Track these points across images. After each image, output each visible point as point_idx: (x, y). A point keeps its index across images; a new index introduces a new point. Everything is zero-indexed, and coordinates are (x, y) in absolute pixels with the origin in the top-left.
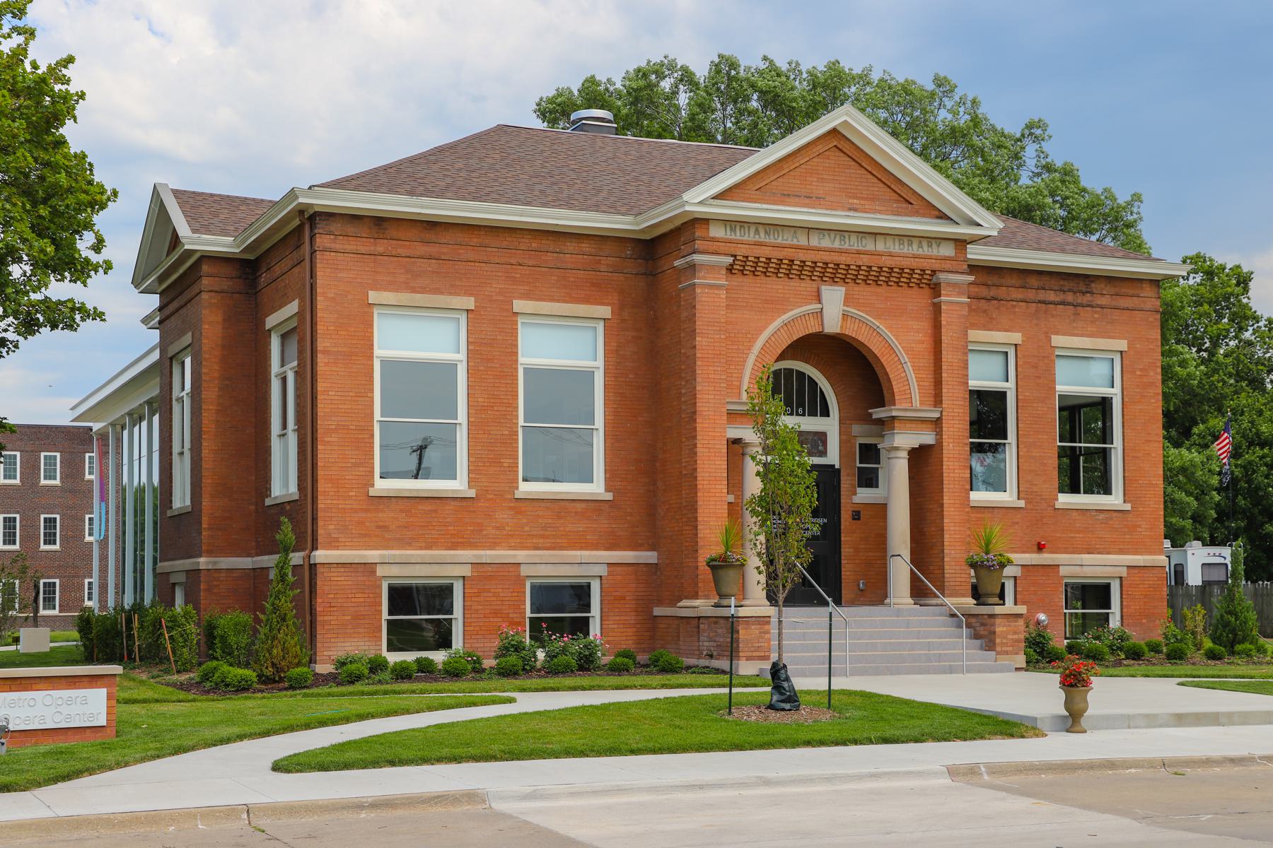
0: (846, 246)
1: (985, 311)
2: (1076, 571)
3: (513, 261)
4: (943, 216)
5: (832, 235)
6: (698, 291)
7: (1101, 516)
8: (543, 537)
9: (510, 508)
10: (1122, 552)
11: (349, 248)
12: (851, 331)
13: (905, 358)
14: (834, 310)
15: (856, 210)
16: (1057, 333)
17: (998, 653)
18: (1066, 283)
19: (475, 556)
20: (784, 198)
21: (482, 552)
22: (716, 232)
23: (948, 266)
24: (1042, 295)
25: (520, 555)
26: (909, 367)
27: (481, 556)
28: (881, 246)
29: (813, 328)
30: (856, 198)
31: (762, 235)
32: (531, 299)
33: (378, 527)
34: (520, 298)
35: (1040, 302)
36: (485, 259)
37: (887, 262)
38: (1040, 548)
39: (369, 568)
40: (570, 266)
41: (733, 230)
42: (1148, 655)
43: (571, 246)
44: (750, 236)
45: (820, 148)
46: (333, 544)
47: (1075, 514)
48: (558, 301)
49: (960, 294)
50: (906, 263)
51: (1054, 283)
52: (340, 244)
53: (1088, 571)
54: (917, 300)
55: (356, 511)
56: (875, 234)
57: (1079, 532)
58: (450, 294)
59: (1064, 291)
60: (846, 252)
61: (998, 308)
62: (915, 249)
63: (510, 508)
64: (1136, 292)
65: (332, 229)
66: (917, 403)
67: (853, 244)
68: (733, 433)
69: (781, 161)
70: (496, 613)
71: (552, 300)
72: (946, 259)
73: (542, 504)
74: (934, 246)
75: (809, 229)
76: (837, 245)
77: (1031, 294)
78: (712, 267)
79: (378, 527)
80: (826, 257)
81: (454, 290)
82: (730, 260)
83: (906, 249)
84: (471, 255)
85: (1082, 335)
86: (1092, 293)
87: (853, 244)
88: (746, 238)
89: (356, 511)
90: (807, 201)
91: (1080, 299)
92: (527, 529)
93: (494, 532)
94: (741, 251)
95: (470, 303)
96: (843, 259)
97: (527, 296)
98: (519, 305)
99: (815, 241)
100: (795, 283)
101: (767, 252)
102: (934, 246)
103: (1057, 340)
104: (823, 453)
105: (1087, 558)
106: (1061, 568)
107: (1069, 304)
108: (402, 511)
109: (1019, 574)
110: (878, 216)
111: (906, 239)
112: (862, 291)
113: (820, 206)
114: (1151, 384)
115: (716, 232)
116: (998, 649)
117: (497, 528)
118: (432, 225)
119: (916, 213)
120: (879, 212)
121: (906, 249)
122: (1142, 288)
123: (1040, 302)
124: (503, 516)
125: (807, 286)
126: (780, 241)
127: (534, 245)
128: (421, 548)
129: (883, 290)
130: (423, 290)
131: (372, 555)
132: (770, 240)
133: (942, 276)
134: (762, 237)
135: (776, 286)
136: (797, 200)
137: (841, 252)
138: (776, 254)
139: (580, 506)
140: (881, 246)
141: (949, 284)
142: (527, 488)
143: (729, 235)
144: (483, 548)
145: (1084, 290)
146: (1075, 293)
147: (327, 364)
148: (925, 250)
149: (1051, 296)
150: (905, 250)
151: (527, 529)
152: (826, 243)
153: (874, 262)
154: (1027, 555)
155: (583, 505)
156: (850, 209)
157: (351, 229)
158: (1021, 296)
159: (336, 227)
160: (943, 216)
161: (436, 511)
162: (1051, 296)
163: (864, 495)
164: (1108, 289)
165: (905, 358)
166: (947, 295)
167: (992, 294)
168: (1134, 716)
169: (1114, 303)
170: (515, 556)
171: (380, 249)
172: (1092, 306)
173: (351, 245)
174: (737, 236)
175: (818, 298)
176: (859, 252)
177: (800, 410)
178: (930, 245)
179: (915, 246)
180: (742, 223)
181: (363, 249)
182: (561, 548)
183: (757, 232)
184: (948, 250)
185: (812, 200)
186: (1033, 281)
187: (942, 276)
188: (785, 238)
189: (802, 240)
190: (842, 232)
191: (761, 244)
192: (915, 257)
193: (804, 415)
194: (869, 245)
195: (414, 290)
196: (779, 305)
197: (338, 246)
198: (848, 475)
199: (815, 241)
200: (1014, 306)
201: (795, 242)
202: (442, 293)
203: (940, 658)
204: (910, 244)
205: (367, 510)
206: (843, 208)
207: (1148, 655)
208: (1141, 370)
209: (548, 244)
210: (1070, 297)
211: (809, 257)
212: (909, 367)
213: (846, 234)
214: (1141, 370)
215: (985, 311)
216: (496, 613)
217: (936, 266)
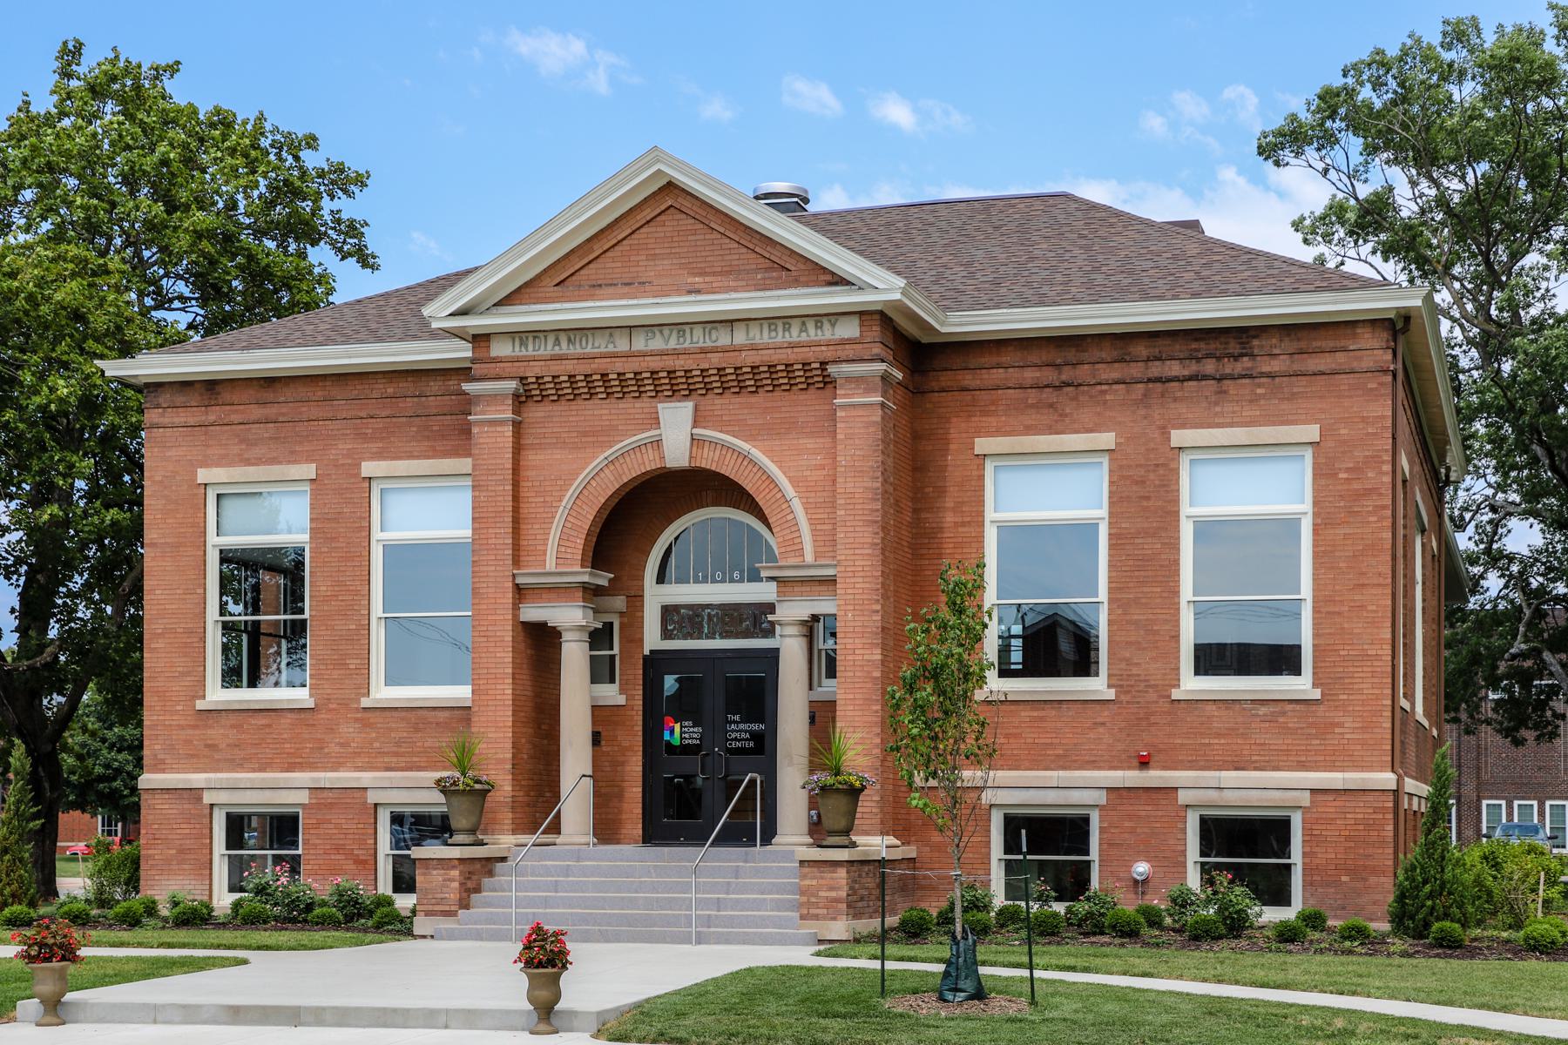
0: (686, 345)
1: (1051, 406)
2: (1213, 795)
3: (363, 414)
4: (837, 280)
5: (666, 331)
6: (475, 430)
7: (1263, 710)
8: (396, 754)
9: (356, 720)
10: (1302, 766)
11: (177, 420)
12: (708, 460)
13: (790, 491)
14: (676, 436)
15: (698, 292)
16: (1183, 426)
18: (1202, 345)
19: (313, 779)
20: (595, 289)
21: (322, 775)
22: (500, 349)
23: (849, 351)
24: (1156, 369)
25: (365, 778)
26: (797, 505)
27: (318, 779)
28: (740, 337)
29: (649, 463)
30: (701, 274)
31: (564, 344)
32: (385, 458)
33: (207, 746)
34: (372, 459)
35: (1150, 380)
36: (330, 415)
37: (749, 358)
38: (1144, 763)
39: (195, 793)
40: (434, 411)
41: (523, 343)
42: (1146, 931)
43: (435, 386)
44: (548, 348)
45: (648, 213)
46: (160, 767)
47: (1210, 708)
48: (418, 457)
49: (868, 391)
51: (1179, 348)
52: (171, 417)
53: (1231, 797)
54: (806, 405)
55: (181, 727)
56: (730, 323)
57: (1218, 735)
58: (289, 462)
59: (1198, 360)
61: (1075, 399)
62: (795, 335)
63: (356, 720)
64: (1343, 343)
65: (161, 400)
66: (809, 557)
67: (699, 339)
68: (531, 613)
69: (589, 240)
70: (338, 849)
71: (411, 457)
72: (843, 342)
73: (395, 714)
74: (827, 326)
75: (630, 329)
76: (673, 344)
77: (1135, 370)
78: (494, 398)
79: (207, 746)
80: (655, 363)
81: (294, 458)
83: (781, 337)
84: (315, 412)
85: (1231, 425)
86: (1252, 356)
87: (699, 339)
89: (181, 727)
90: (626, 289)
91: (1229, 367)
92: (377, 745)
93: (337, 749)
94: (532, 372)
95: (310, 470)
96: (680, 363)
97: (380, 455)
98: (368, 468)
99: (640, 343)
100: (628, 405)
101: (570, 367)
102: (827, 326)
103: (1179, 437)
105: (1229, 777)
106: (1180, 792)
107: (1205, 377)
108: (233, 726)
109: (1103, 801)
110: (734, 295)
111: (780, 323)
112: (716, 403)
113: (645, 294)
114: (1368, 492)
115: (500, 349)
117: (342, 745)
118: (270, 382)
119: (796, 283)
120: (735, 290)
121: (781, 337)
122: (1355, 336)
123: (1150, 380)
124: (348, 730)
125: (644, 404)
126: (589, 350)
127: (390, 390)
128: (254, 771)
129: (760, 399)
130: (258, 462)
131: (197, 779)
132: (576, 350)
133: (831, 369)
134: (564, 348)
135: (599, 411)
136: (611, 290)
137: (676, 353)
138: (582, 369)
139: (442, 715)
140: (740, 337)
141: (849, 379)
142: (383, 693)
143: (519, 352)
144: (325, 769)
145: (1237, 352)
146: (1219, 359)
147: (154, 559)
148: (812, 334)
149: (1175, 369)
150: (779, 339)
151: (377, 745)
152: (657, 343)
153: (729, 361)
154: (1119, 773)
155: (447, 714)
156: (690, 292)
157: (180, 399)
158: (1115, 375)
159: (164, 398)
160: (837, 280)
161: (269, 726)
162: (1175, 369)
163: (610, 694)
164: (1289, 345)
165: (790, 491)
166: (845, 396)
167: (1064, 377)
168: (163, 1006)
169: (1296, 367)
170: (358, 779)
171: (212, 418)
172: (1251, 377)
173: (181, 417)
174: (530, 351)
175: (656, 422)
176: (704, 351)
177: (736, 575)
178: (819, 326)
179: (795, 331)
180: (537, 333)
181: (192, 421)
182: (419, 769)
183: (557, 342)
184: (849, 329)
185: (633, 286)
186: (1141, 350)
187: (831, 369)
188: (599, 345)
189: (622, 345)
190: (680, 326)
191: (560, 358)
192: (792, 346)
193: (741, 580)
194: (723, 338)
195: (248, 462)
196: (600, 436)
197: (166, 421)
199: (640, 343)
200: (1104, 392)
201: (611, 348)
202: (280, 463)
203: (731, 922)
204: (787, 328)
205: (195, 727)
206: (679, 292)
207: (1146, 931)
208: (1348, 470)
209: (406, 386)
210: (1209, 367)
211: (629, 367)
212: (797, 505)
213: (687, 328)
214: (1348, 470)
215: (1051, 406)
216: (338, 849)
217: (828, 354)
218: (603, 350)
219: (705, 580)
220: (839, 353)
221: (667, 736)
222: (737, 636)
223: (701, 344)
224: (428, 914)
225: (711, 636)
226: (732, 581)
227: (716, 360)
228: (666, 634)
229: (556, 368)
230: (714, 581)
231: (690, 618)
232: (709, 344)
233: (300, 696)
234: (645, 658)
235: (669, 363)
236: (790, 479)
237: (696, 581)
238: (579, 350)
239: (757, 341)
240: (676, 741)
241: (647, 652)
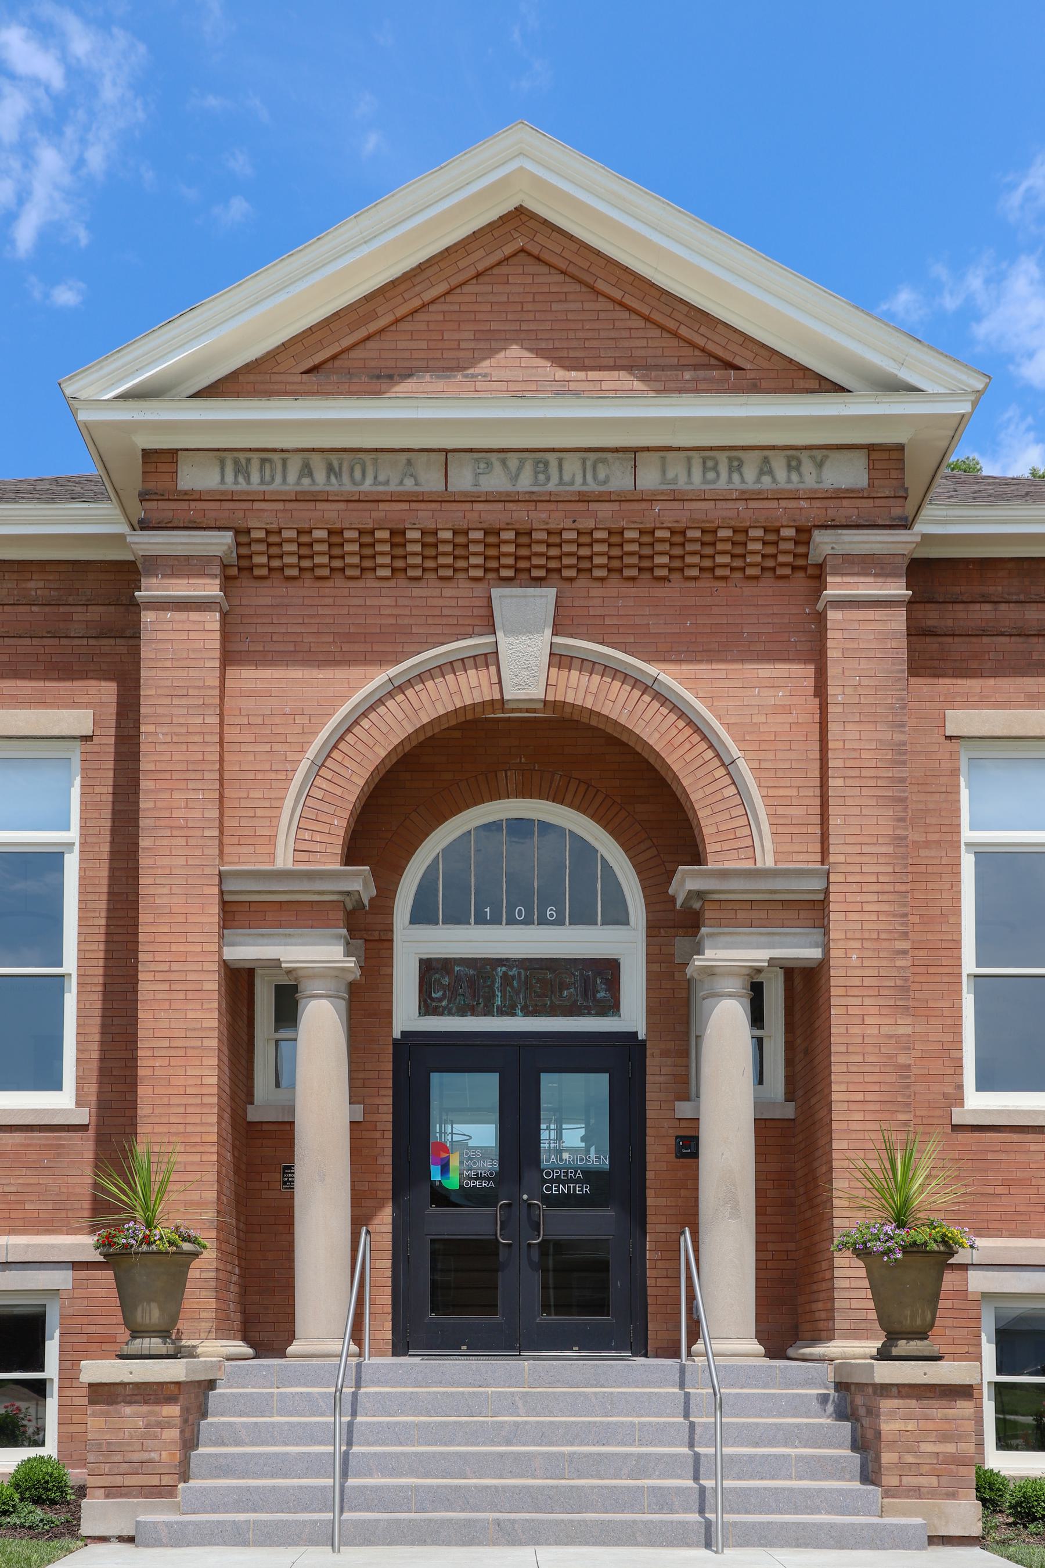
0: (551, 486)
17: (888, 1493)
29: (471, 689)
37: (671, 515)
50: (719, 513)
60: (551, 499)
80: (493, 515)
82: (228, 537)
88: (277, 485)
94: (259, 521)
96: (540, 517)
101: (332, 514)
104: (611, 1007)
116: (890, 1480)
126: (367, 486)
137: (533, 500)
152: (496, 481)
176: (584, 498)
192: (746, 497)
198: (665, 1054)
218: (393, 487)
219: (496, 921)
220: (831, 513)
221: (436, 1175)
222: (553, 1011)
223: (578, 487)
224: (112, 1492)
225: (508, 1011)
226: (543, 921)
227: (605, 511)
228: (427, 1006)
229: (304, 515)
230: (511, 921)
231: (472, 982)
232: (592, 487)
233: (488, 910)
234: (396, 1043)
235: (520, 515)
236: (728, 726)
237: (481, 920)
238: (348, 487)
239: (682, 484)
240: (453, 1182)
241: (397, 1034)
